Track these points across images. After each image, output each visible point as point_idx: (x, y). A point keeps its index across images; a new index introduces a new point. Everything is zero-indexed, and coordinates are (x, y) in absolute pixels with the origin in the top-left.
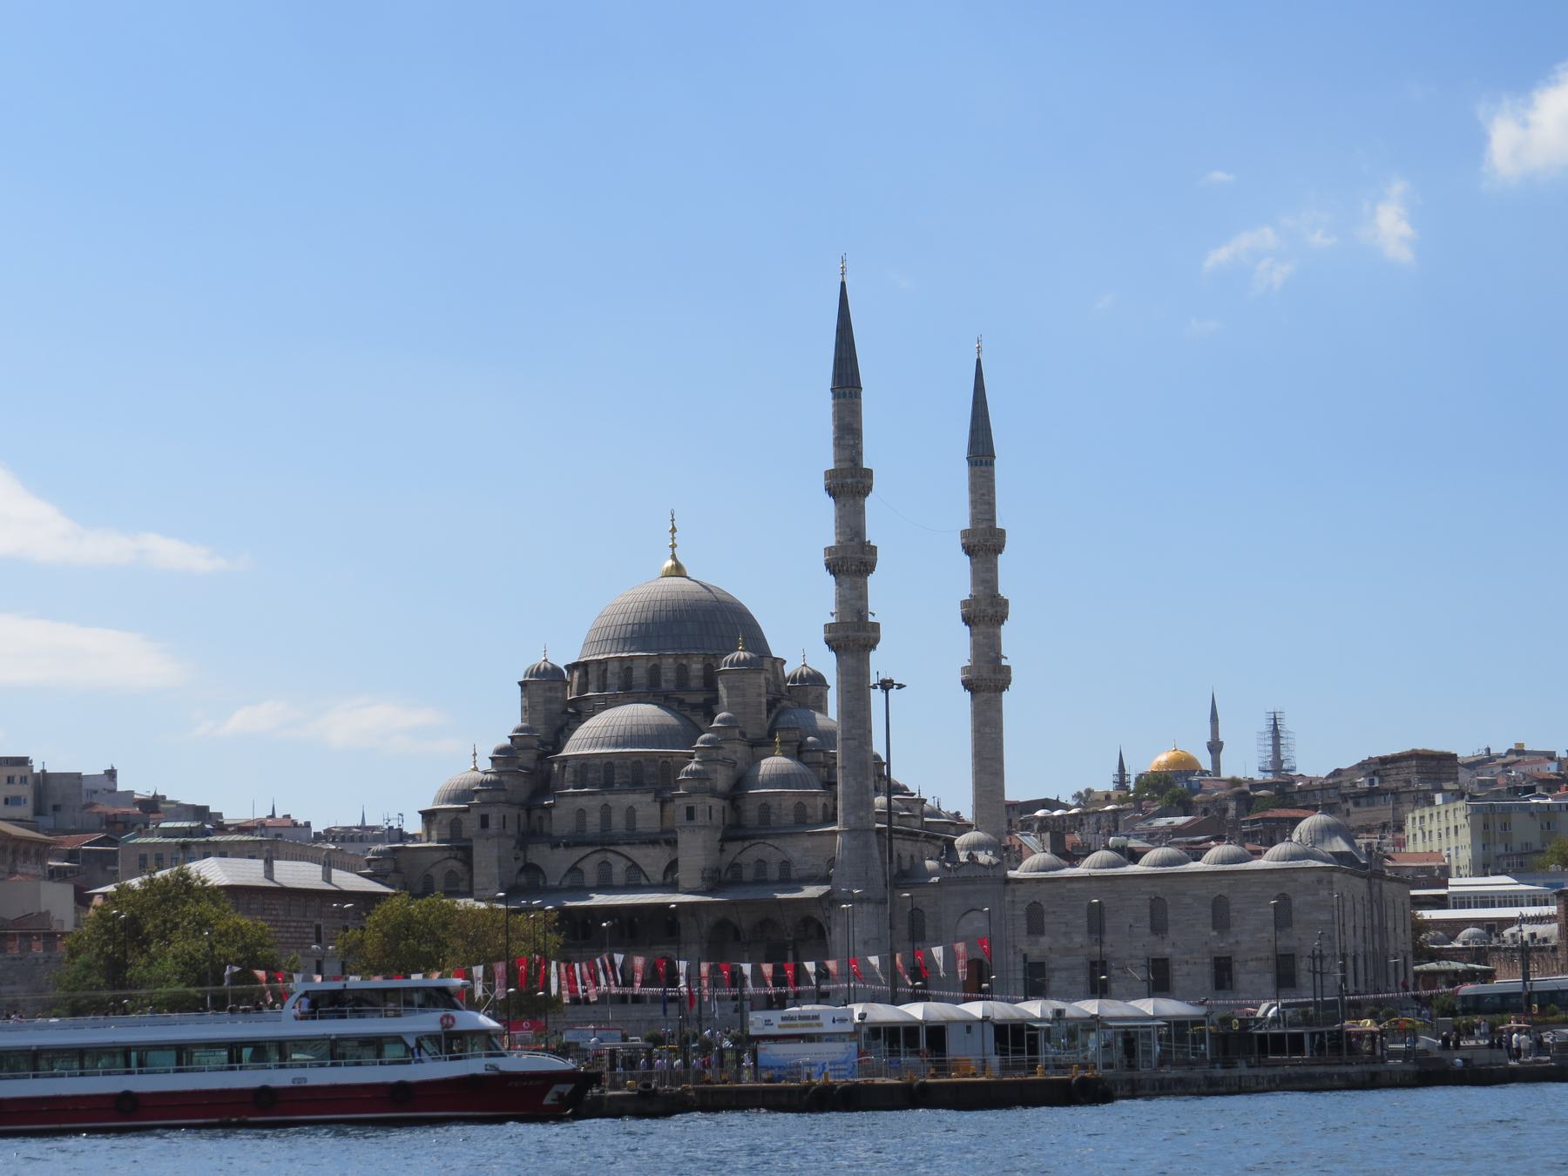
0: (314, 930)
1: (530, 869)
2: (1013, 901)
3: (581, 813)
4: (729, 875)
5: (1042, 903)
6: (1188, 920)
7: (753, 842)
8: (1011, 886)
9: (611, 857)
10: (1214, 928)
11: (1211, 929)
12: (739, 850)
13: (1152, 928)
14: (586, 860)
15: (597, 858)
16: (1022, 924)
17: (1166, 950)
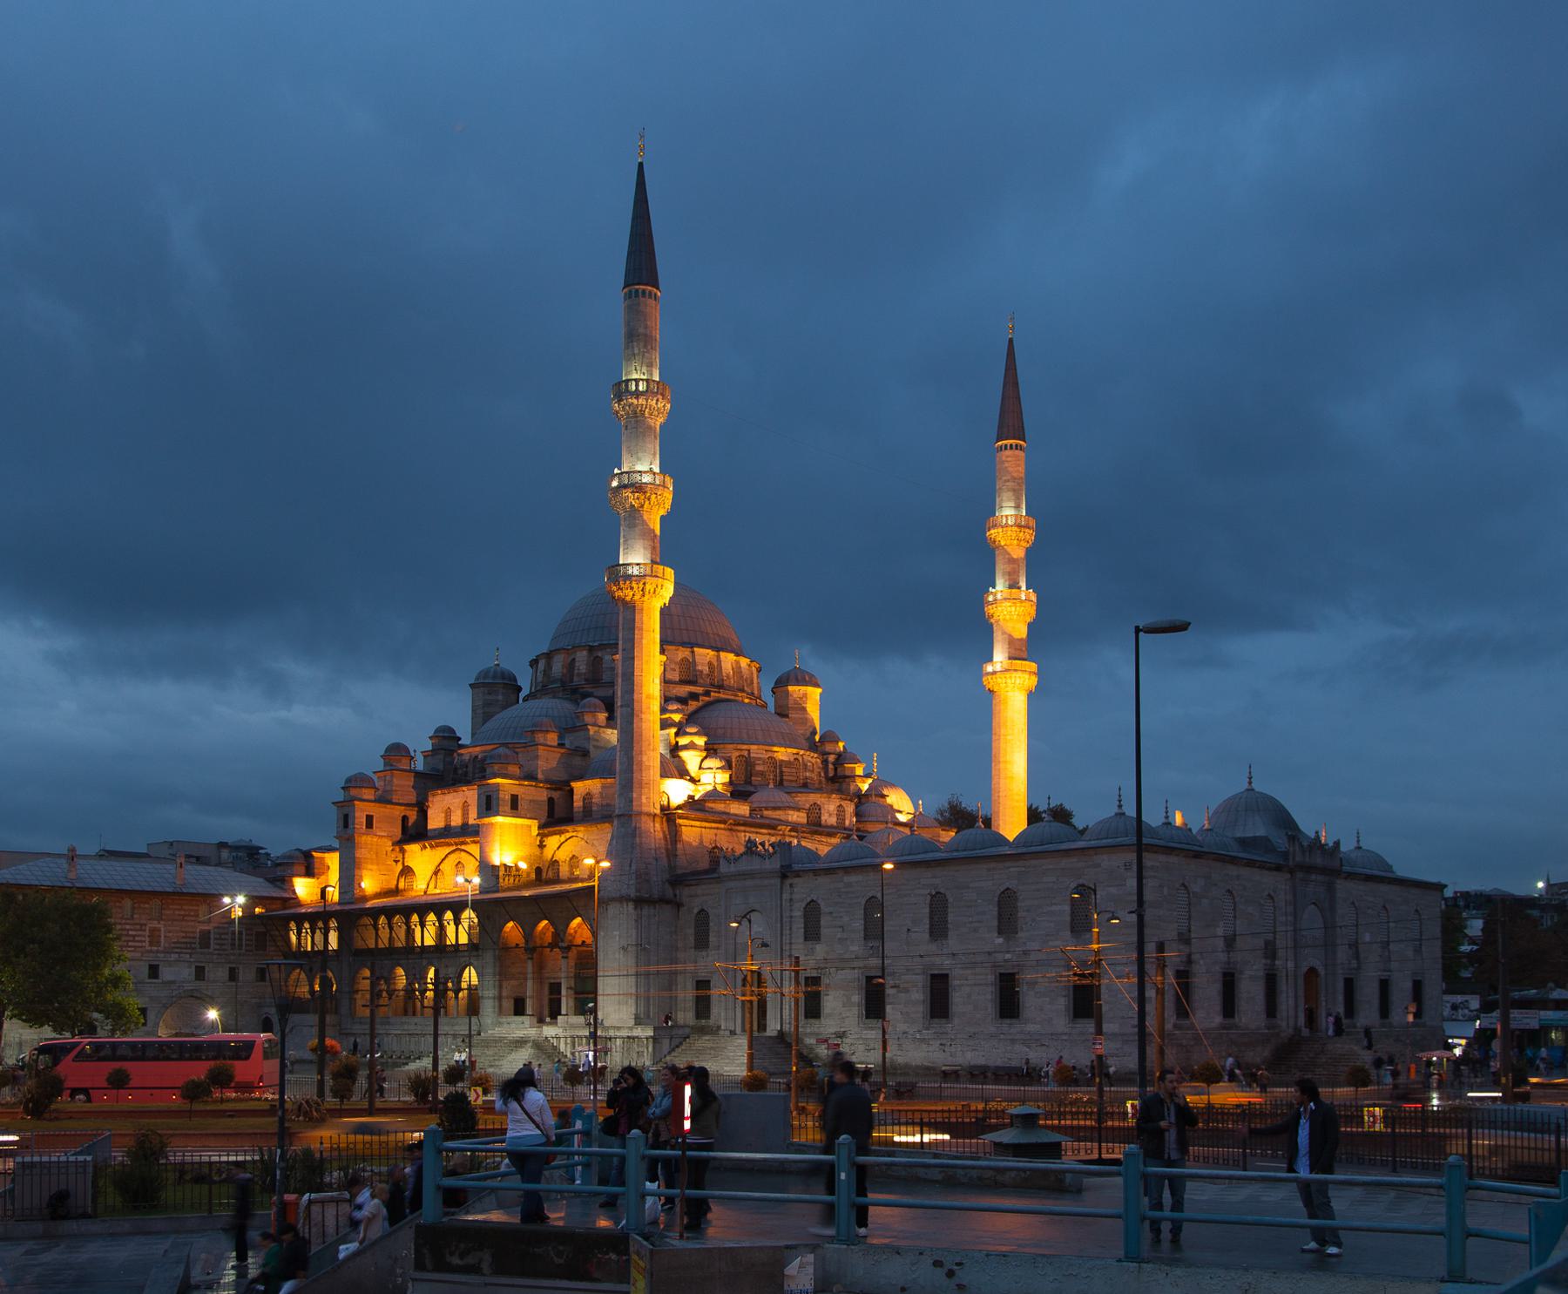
0: (147, 933)
1: (407, 871)
2: (791, 900)
3: (448, 813)
4: (550, 874)
5: (819, 902)
6: (972, 922)
7: (568, 835)
8: (788, 881)
9: (463, 854)
10: (1000, 932)
11: (996, 935)
12: (557, 846)
13: (931, 933)
14: (446, 861)
15: (454, 858)
16: (799, 927)
17: (944, 964)
